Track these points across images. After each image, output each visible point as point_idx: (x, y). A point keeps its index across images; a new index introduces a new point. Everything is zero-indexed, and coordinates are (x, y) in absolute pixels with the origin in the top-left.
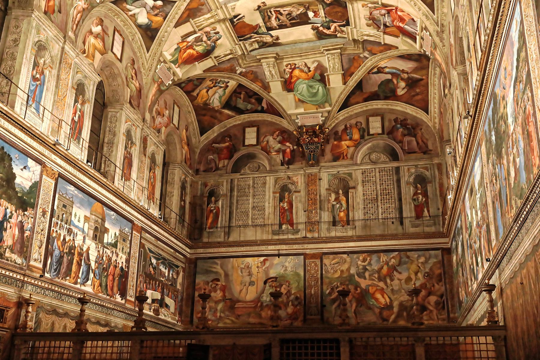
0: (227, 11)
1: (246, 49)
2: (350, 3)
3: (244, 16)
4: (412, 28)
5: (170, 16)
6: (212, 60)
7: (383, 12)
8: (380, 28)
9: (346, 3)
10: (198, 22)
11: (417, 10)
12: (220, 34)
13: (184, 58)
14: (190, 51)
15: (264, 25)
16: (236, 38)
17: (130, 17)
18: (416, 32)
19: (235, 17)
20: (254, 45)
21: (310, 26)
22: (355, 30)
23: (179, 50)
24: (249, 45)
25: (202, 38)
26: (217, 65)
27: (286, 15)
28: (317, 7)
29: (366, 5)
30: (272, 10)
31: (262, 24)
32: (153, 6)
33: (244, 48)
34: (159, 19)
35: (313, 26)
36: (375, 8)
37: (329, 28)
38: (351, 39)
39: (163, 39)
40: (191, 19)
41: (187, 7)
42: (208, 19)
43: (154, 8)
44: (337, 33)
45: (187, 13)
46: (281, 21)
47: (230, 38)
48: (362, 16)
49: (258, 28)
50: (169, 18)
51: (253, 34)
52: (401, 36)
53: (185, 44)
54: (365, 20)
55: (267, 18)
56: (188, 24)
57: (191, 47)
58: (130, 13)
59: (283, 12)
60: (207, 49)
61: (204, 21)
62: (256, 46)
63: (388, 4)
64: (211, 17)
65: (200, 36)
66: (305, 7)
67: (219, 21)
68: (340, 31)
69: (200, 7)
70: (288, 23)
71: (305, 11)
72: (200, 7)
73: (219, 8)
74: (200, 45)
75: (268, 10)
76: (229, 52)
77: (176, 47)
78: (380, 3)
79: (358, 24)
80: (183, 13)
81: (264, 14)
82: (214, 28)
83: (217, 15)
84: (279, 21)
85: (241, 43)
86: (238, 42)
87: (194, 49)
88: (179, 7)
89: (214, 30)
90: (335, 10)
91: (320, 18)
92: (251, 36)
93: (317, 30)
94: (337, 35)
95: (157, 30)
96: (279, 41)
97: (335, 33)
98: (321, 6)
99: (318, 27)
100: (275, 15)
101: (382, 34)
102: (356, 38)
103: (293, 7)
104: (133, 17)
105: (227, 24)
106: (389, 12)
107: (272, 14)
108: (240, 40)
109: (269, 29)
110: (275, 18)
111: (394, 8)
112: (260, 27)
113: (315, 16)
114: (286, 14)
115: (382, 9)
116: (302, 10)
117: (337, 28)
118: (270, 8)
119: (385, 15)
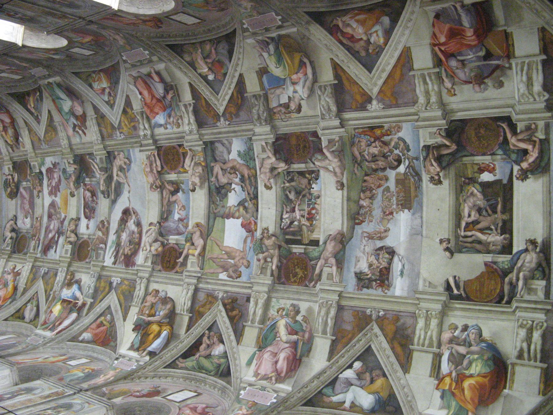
0: (431, 295)
1: (536, 302)
2: (453, 114)
3: (455, 277)
4: (459, 16)
5: (386, 367)
6: (522, 365)
7: (453, 63)
8: (498, 67)
9: (452, 121)
10: (421, 341)
11: (415, 15)
12: (470, 325)
13: (471, 399)
14: (466, 384)
15: (492, 255)
16: (496, 306)
17: (352, 409)
18: (459, 8)
19: (448, 288)
20: (534, 287)
21: (516, 183)
22: (518, 108)
23: (448, 394)
24: (529, 294)
25: (458, 353)
26: (545, 366)
27: (480, 215)
28: (469, 166)
29: (449, 91)
30: (463, 234)
31: (489, 258)
32: (357, 375)
33: (533, 306)
34: (380, 382)
35: (517, 179)
36: (452, 76)
37: (525, 152)
38: (549, 114)
39: (409, 399)
40: (411, 347)
41: (388, 338)
42: (427, 325)
43: (360, 375)
44: (534, 139)
45: (396, 345)
46: (493, 227)
47: (490, 315)
48: (479, 96)
49: (495, 267)
50: (388, 370)
51: (507, 280)
52: (500, 29)
53: (447, 380)
54: (487, 92)
55: (478, 246)
56: (415, 355)
57: (461, 378)
58: (347, 405)
59: (473, 218)
60: (489, 359)
61: (426, 333)
62: (540, 284)
63: (433, 58)
64: (426, 320)
65: (451, 354)
66: (469, 184)
67: (443, 314)
68: (529, 132)
69: (399, 324)
70: (500, 217)
71: (478, 186)
72: (399, 324)
73: (417, 302)
74: (470, 363)
75: (461, 239)
76: (523, 333)
77: (438, 394)
78: (437, 70)
79: (501, 102)
80: (393, 349)
81: (466, 247)
82: (453, 327)
83: (427, 311)
84: (491, 230)
85: (514, 304)
86: (511, 308)
87: (471, 376)
88: (381, 348)
89: (456, 328)
90: (474, 139)
91: (495, 163)
92: (511, 283)
93: (528, 173)
94: (540, 140)
95: (392, 396)
96: (539, 240)
97: (535, 142)
98: (465, 159)
99: (522, 169)
100: (473, 232)
101: (513, 62)
102: (543, 105)
103: (465, 201)
104: (354, 406)
105: (458, 306)
106: (449, 55)
107: (471, 236)
108: (509, 302)
109: (507, 248)
110: (482, 233)
111: (436, 48)
112: (495, 263)
113: (492, 171)
114: (477, 215)
115: (449, 67)
116: (475, 190)
117: (520, 137)
118: (457, 237)
119: (463, 61)
